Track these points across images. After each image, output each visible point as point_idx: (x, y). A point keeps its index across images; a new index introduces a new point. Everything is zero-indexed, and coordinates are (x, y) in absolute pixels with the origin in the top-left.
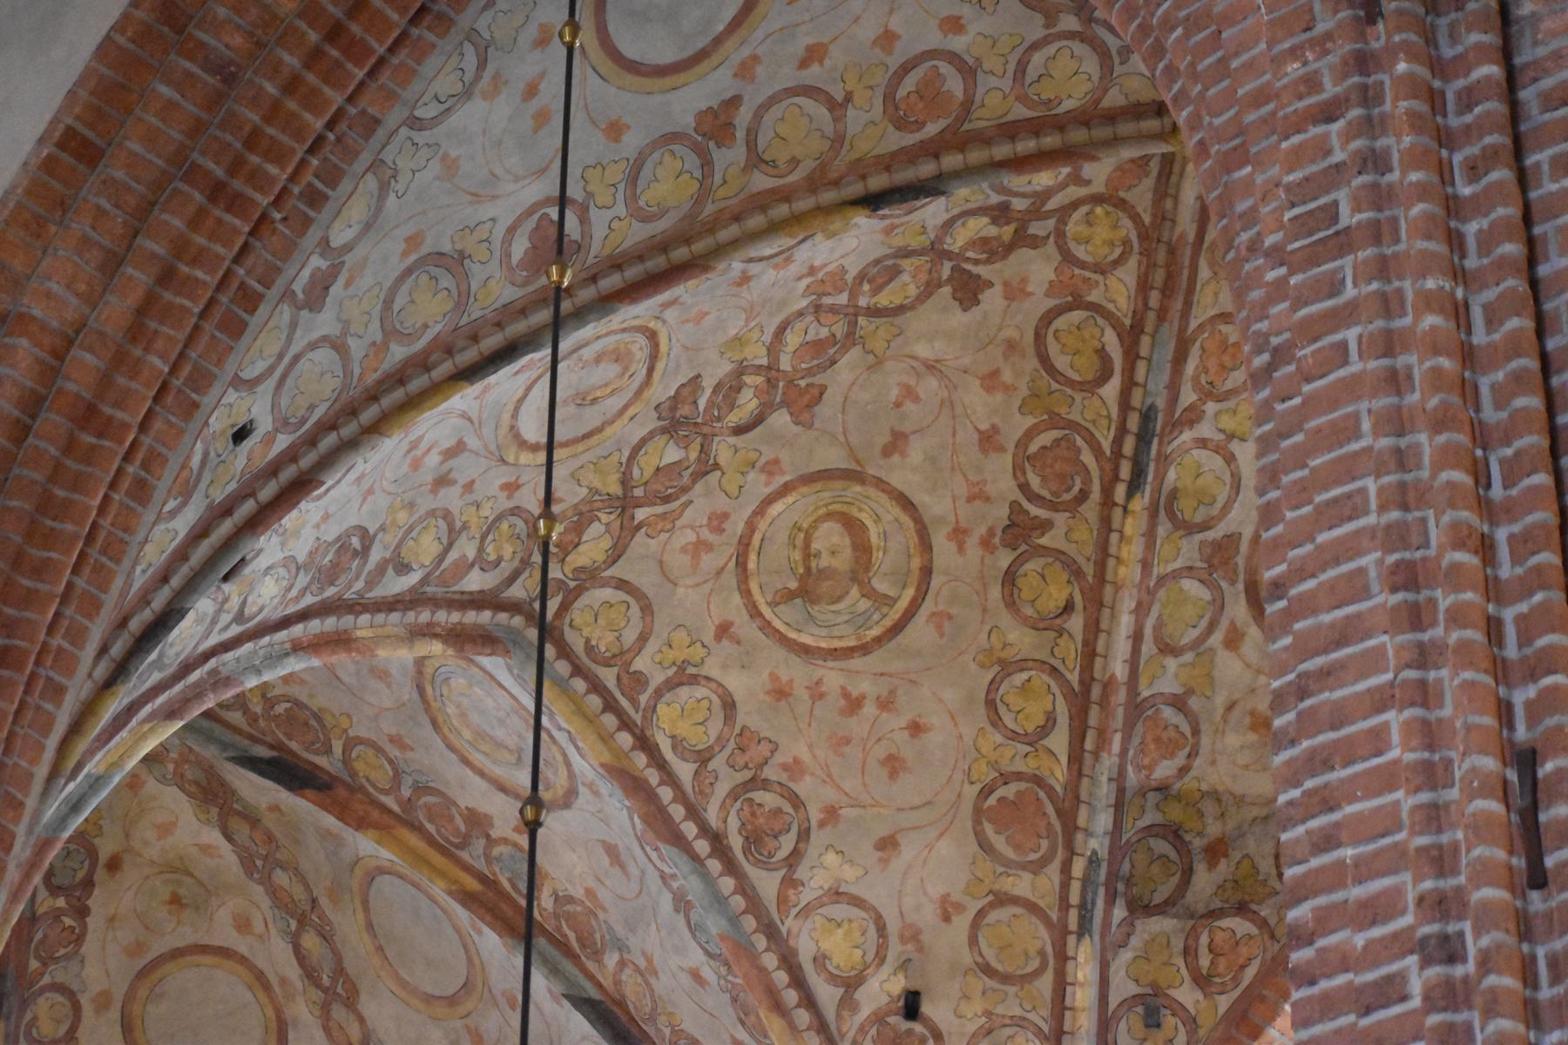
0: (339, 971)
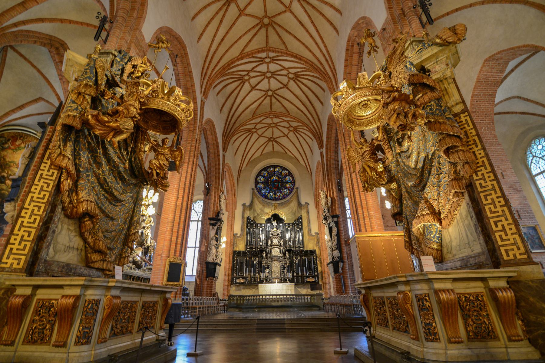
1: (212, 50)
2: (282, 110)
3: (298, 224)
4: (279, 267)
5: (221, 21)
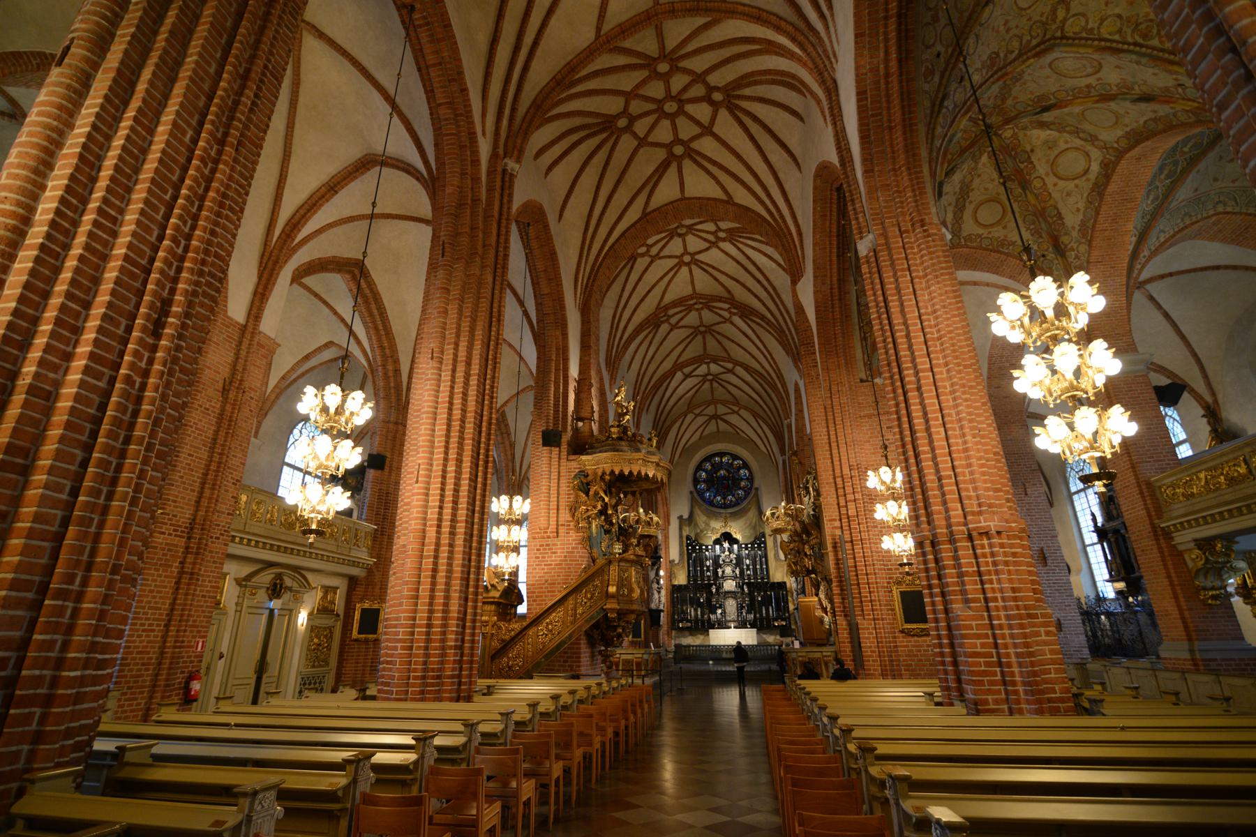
0: (1091, 135)
1: (642, 372)
2: (728, 397)
3: (759, 545)
5: (651, 343)
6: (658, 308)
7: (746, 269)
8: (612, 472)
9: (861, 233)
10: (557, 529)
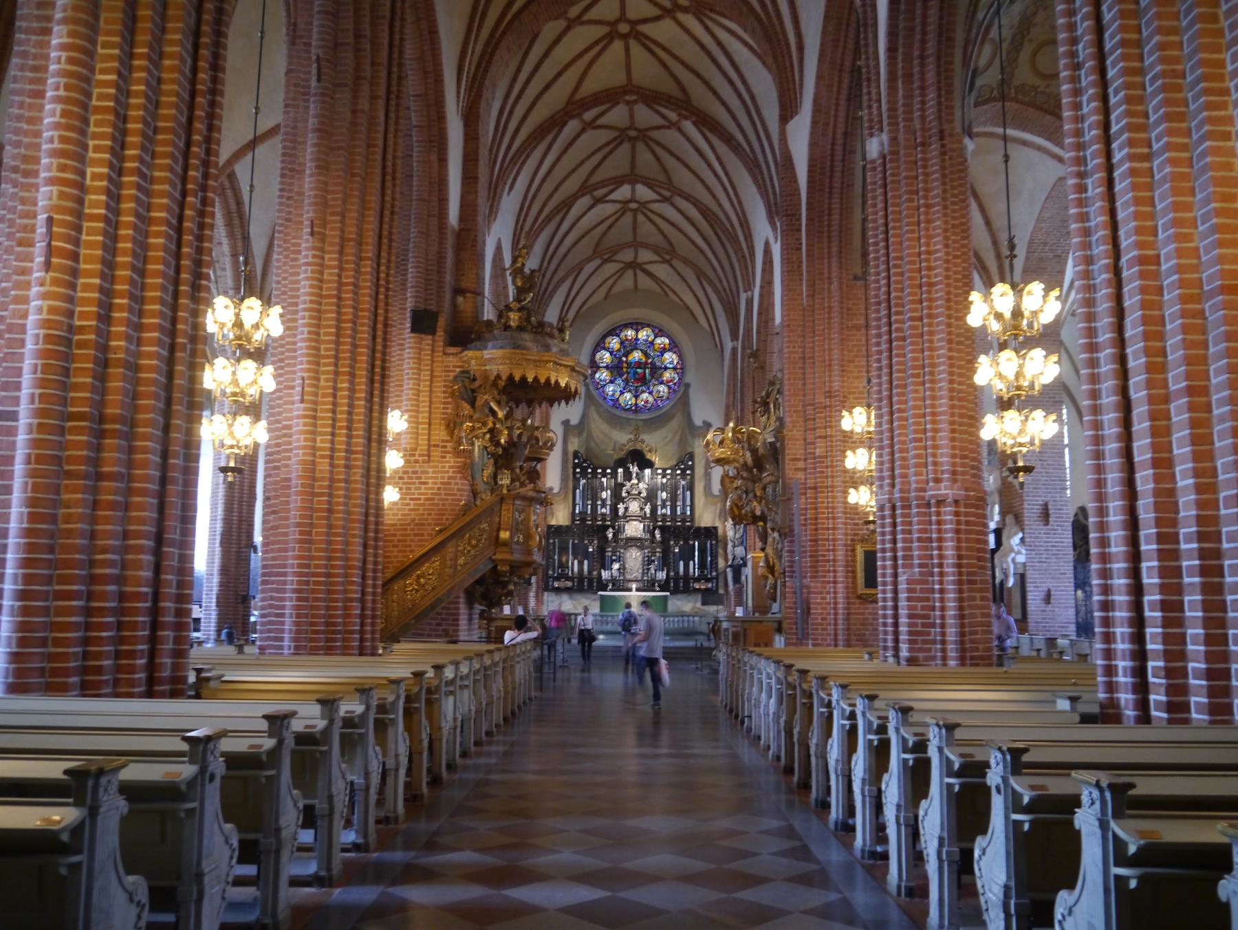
3: (683, 471)
4: (640, 559)
6: (570, 102)
7: (714, 60)
8: (511, 378)
9: (871, 128)
10: (429, 450)
